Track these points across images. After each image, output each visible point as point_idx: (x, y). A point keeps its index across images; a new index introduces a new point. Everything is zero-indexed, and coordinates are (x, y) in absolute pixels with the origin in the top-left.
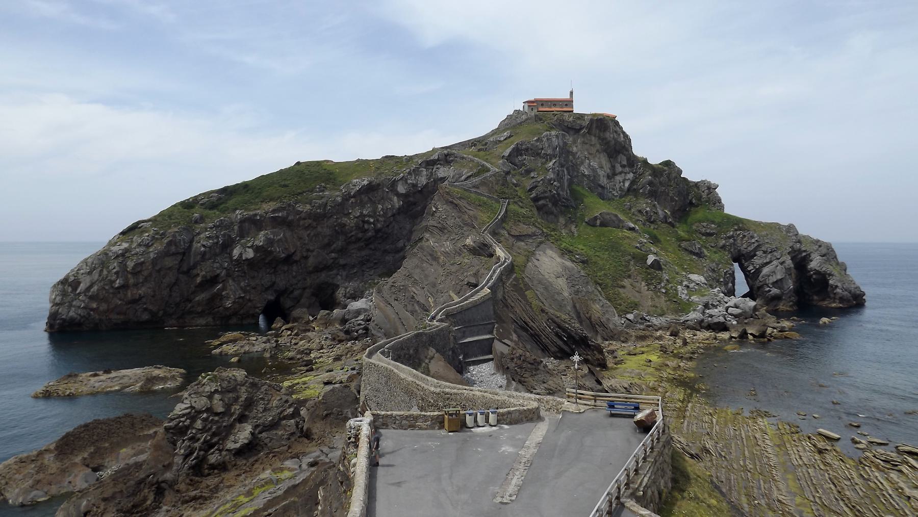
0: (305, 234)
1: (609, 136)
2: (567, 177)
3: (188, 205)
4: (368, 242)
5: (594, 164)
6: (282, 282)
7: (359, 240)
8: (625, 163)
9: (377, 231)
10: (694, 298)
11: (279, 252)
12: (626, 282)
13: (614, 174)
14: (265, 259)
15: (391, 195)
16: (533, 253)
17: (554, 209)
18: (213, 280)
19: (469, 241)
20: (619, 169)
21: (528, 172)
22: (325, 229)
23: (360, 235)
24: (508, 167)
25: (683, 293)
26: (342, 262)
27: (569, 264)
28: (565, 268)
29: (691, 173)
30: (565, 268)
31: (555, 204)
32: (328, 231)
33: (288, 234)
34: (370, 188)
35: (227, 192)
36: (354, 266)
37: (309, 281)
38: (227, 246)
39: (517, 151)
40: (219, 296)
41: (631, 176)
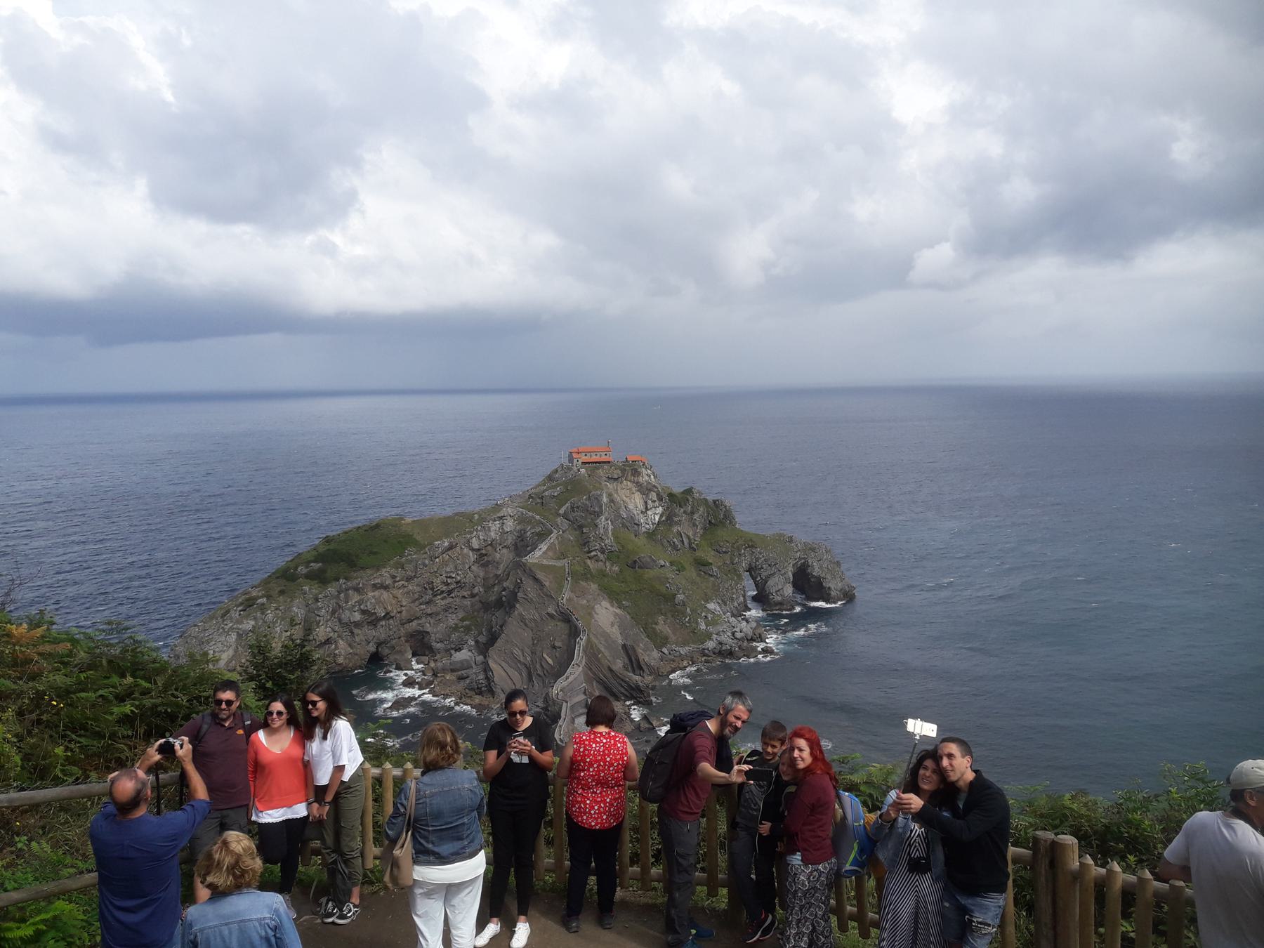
0: (399, 593)
1: (644, 479)
4: (450, 592)
6: (381, 632)
7: (442, 592)
8: (655, 498)
9: (457, 583)
10: (710, 629)
12: (661, 619)
13: (647, 509)
15: (466, 550)
17: (602, 556)
19: (551, 610)
20: (650, 504)
21: (581, 527)
23: (445, 588)
24: (565, 524)
25: (703, 626)
26: (429, 611)
27: (618, 611)
28: (616, 615)
30: (616, 615)
31: (603, 552)
32: (419, 589)
33: (385, 595)
36: (438, 614)
37: (403, 631)
41: (660, 510)
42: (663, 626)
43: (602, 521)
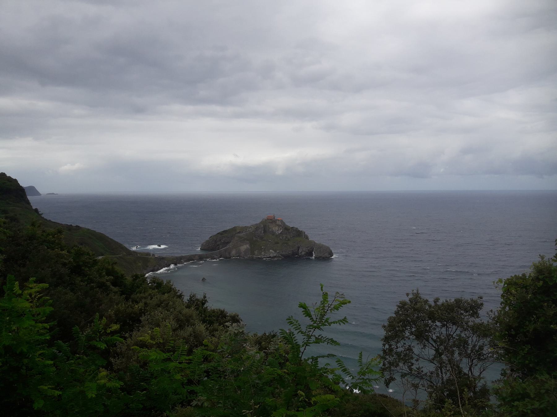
25: (263, 253)
42: (256, 252)
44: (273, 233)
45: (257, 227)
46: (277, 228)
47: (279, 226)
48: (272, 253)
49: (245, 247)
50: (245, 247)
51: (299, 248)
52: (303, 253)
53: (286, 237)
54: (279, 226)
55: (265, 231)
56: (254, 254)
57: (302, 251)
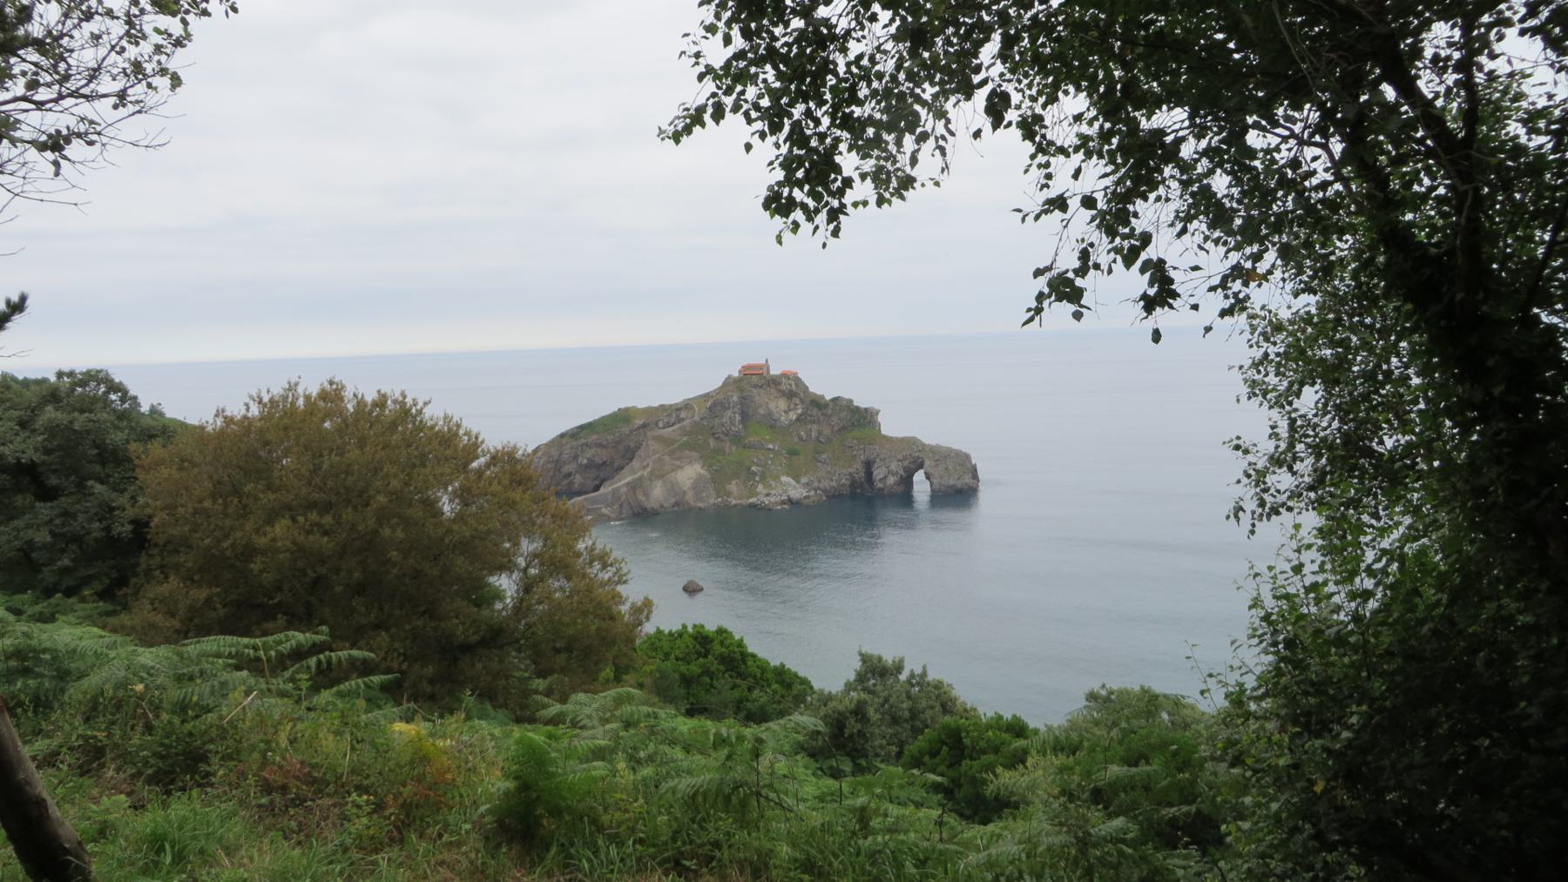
1: (783, 387)
2: (738, 418)
3: (562, 436)
5: (772, 405)
11: (598, 460)
14: (592, 465)
16: (681, 468)
18: (570, 474)
22: (621, 448)
25: (760, 488)
29: (861, 402)
34: (644, 426)
35: (582, 427)
38: (576, 457)
39: (714, 404)
40: (571, 483)
42: (733, 487)
43: (729, 413)
44: (771, 423)
45: (714, 404)
46: (782, 404)
47: (790, 395)
48: (794, 488)
49: (689, 474)
50: (689, 474)
51: (868, 465)
52: (891, 480)
53: (820, 433)
54: (790, 395)
55: (745, 418)
56: (729, 494)
57: (886, 475)
